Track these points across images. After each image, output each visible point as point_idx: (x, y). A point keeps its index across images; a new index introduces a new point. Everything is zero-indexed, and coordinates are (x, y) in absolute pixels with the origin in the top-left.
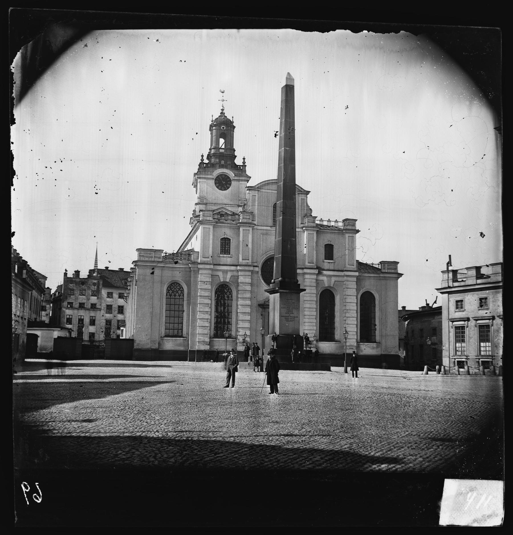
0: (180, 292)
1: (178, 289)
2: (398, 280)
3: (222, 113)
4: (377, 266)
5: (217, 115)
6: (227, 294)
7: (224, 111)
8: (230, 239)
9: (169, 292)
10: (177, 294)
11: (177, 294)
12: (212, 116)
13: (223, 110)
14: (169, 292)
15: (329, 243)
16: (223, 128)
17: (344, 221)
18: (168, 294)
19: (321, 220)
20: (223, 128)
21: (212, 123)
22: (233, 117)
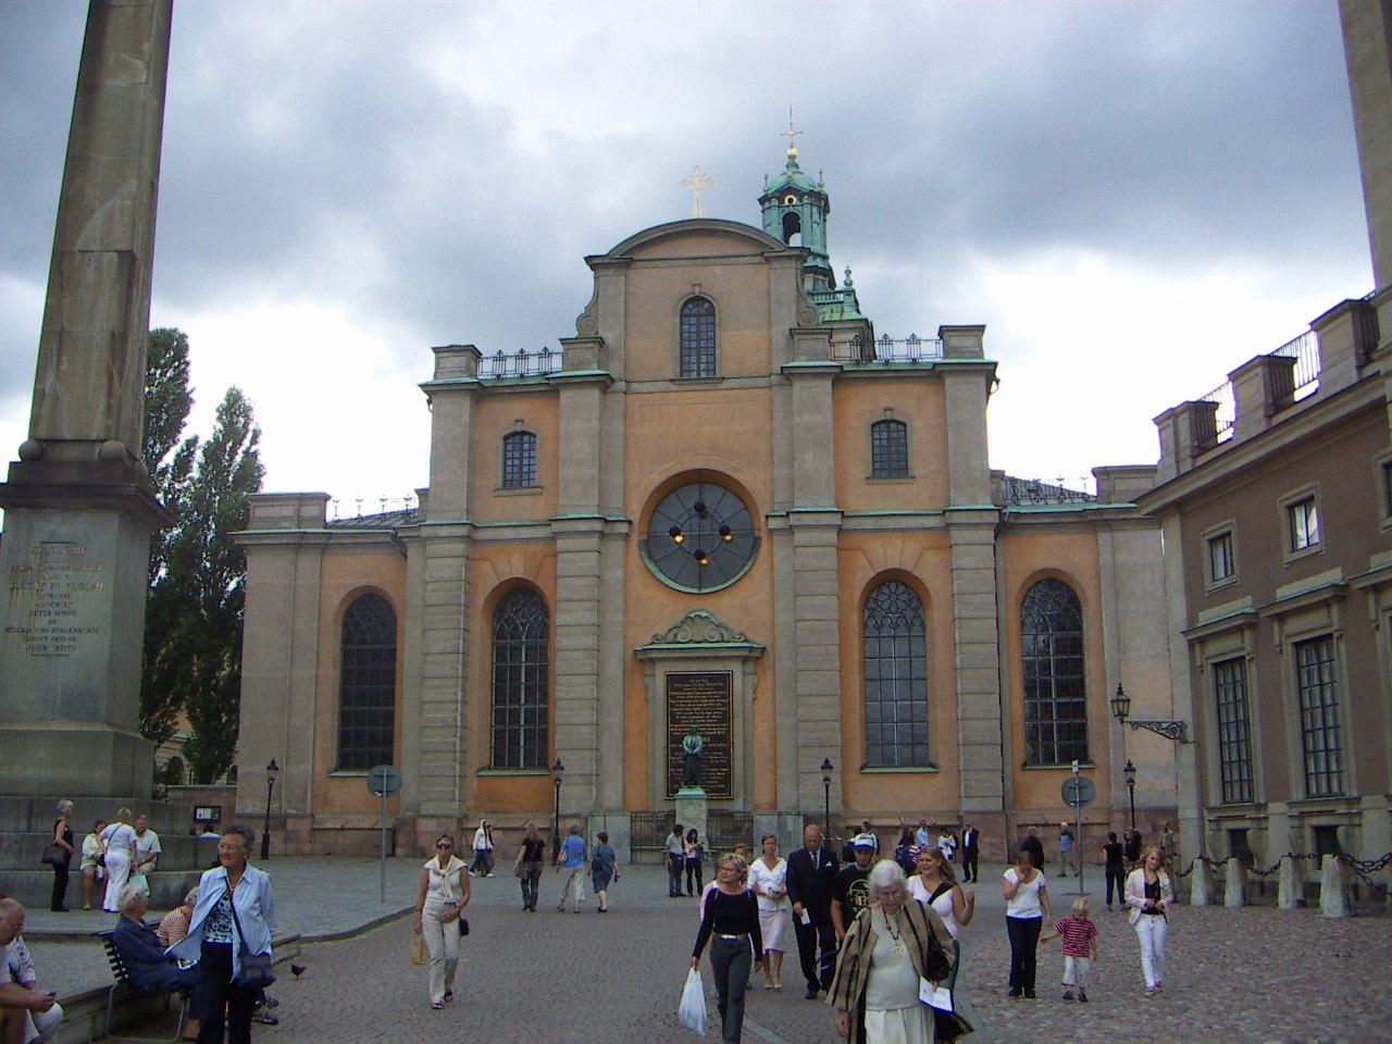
3: (792, 163)
8: (534, 436)
12: (766, 178)
15: (889, 416)
16: (790, 200)
20: (790, 200)
21: (764, 194)
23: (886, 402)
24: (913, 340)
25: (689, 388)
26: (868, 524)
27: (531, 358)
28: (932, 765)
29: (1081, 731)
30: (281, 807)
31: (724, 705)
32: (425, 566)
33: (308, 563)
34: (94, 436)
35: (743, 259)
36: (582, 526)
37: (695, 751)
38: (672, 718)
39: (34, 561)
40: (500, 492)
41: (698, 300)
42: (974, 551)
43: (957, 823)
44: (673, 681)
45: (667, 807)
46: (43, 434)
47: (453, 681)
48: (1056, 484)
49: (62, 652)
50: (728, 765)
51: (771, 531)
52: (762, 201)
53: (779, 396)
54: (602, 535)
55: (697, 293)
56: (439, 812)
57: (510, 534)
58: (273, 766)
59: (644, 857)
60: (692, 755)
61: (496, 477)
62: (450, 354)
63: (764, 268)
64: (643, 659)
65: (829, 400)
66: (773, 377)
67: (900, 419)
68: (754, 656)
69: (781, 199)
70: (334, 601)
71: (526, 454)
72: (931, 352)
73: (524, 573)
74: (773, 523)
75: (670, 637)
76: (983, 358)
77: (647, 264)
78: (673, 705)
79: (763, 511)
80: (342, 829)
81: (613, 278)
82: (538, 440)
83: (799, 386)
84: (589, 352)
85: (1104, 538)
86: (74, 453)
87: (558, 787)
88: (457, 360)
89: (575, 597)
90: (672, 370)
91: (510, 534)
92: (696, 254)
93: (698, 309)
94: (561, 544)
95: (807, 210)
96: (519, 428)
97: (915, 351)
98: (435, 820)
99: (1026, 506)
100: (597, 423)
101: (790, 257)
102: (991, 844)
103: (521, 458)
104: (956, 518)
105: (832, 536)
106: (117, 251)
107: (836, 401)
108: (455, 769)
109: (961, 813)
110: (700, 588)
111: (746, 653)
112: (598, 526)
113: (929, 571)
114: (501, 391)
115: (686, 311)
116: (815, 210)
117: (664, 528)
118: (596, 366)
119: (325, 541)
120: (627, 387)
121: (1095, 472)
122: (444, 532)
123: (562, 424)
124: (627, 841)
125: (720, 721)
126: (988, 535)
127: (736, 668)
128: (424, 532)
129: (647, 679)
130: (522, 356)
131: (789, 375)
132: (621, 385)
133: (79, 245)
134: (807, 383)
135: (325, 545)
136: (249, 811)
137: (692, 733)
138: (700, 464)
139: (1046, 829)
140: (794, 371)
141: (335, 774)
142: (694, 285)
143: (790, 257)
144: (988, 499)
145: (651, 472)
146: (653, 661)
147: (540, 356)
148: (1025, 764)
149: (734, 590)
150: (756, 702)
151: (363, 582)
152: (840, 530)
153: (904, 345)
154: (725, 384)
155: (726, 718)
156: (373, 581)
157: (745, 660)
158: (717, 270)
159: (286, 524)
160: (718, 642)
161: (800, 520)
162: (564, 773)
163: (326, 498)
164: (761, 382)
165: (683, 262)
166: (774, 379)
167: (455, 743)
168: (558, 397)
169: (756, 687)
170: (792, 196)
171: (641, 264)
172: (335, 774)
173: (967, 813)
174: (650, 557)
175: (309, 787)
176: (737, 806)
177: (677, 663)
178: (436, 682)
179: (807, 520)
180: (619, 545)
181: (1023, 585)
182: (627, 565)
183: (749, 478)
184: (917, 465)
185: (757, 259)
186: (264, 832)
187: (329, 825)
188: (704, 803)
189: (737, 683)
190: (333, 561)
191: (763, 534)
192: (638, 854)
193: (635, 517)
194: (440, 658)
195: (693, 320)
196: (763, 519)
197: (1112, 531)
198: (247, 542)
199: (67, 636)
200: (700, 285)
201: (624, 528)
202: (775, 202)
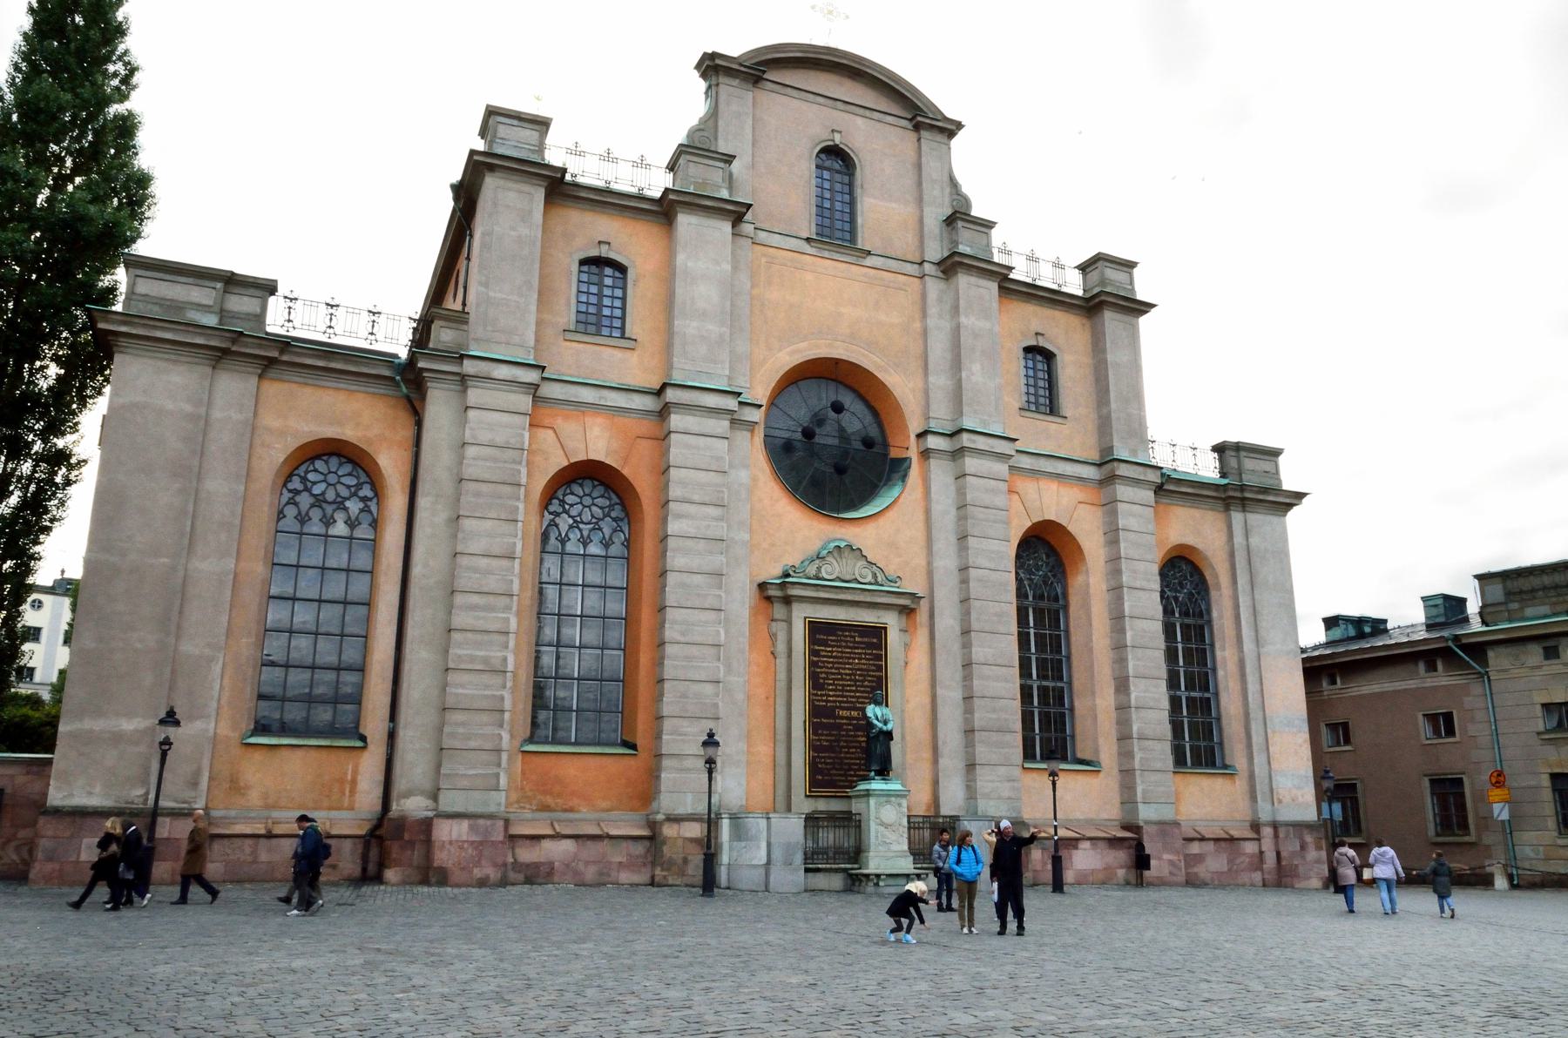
0: (354, 506)
1: (349, 487)
6: (600, 529)
9: (298, 499)
10: (340, 517)
11: (340, 517)
14: (298, 499)
15: (1042, 343)
18: (291, 512)
23: (1036, 326)
24: (1058, 265)
25: (826, 254)
30: (147, 794)
32: (463, 422)
33: (234, 387)
40: (569, 336)
44: (819, 631)
47: (504, 601)
53: (934, 287)
55: (837, 142)
56: (472, 809)
57: (587, 395)
61: (565, 312)
62: (515, 122)
63: (912, 136)
70: (275, 454)
72: (1074, 285)
73: (607, 455)
75: (812, 570)
79: (914, 427)
81: (735, 95)
82: (631, 275)
85: (1237, 517)
88: (528, 133)
89: (696, 498)
90: (808, 230)
91: (587, 395)
93: (836, 158)
94: (676, 420)
96: (604, 252)
98: (465, 824)
102: (1171, 863)
103: (600, 295)
104: (1123, 470)
108: (501, 738)
112: (731, 403)
113: (1085, 527)
114: (583, 194)
119: (275, 354)
121: (1220, 449)
122: (503, 372)
123: (680, 258)
124: (799, 858)
127: (891, 621)
128: (469, 367)
129: (774, 624)
130: (608, 157)
131: (951, 266)
134: (973, 280)
138: (839, 352)
139: (1203, 843)
140: (966, 261)
141: (253, 740)
142: (833, 131)
145: (780, 350)
146: (787, 601)
147: (635, 164)
149: (881, 521)
150: (908, 667)
154: (869, 261)
156: (349, 433)
158: (859, 121)
160: (870, 584)
161: (974, 442)
163: (270, 288)
164: (910, 268)
167: (502, 698)
169: (907, 646)
171: (770, 86)
172: (253, 740)
173: (1147, 822)
175: (206, 763)
177: (818, 607)
178: (475, 599)
179: (982, 443)
183: (901, 384)
189: (894, 638)
190: (276, 390)
191: (913, 454)
194: (484, 562)
197: (1244, 511)
198: (123, 329)
200: (840, 132)
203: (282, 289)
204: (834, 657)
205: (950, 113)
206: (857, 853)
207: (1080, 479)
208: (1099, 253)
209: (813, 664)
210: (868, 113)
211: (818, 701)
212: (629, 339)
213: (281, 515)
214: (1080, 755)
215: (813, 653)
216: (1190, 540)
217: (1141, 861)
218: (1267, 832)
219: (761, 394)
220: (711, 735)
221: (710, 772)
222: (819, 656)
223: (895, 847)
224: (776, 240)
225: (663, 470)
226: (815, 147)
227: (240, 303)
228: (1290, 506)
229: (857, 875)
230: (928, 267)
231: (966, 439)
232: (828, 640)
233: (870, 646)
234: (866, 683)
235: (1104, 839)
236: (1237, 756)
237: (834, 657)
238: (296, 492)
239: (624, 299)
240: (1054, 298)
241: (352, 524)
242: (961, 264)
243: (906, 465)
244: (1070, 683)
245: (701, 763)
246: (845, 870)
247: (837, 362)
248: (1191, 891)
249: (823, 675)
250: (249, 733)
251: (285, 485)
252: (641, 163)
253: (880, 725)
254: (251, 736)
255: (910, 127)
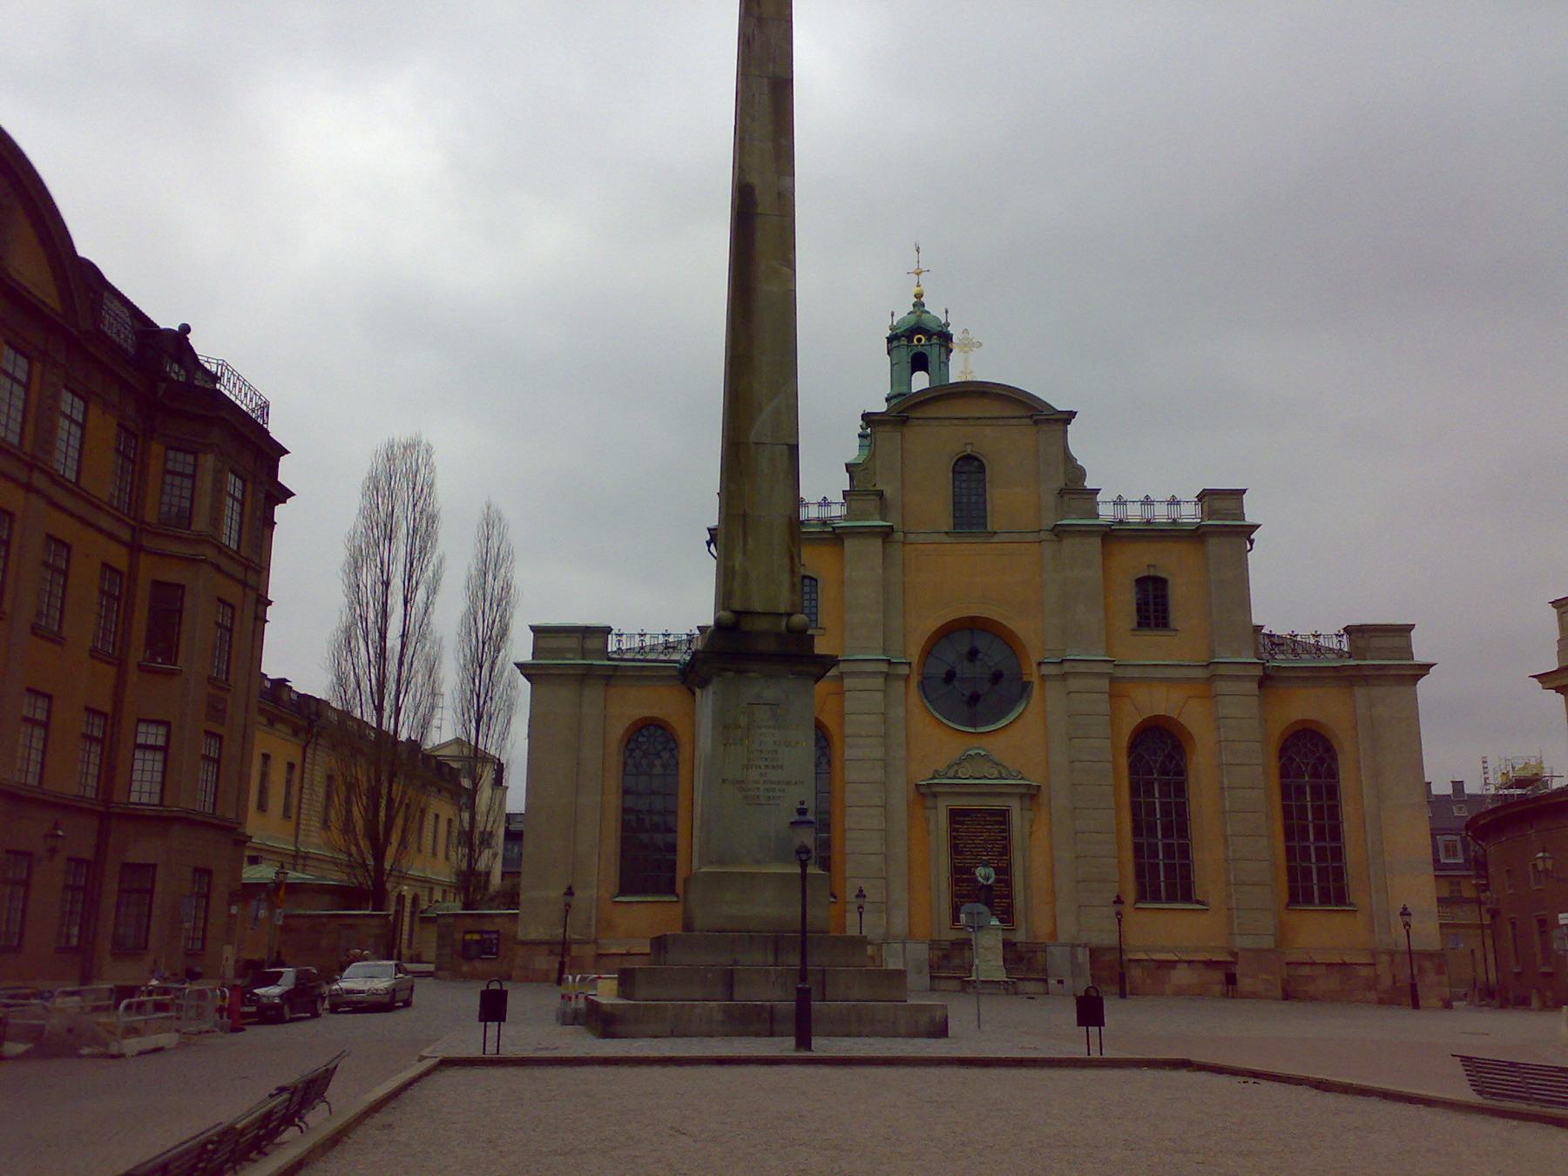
0: (666, 755)
2: (1415, 684)
3: (919, 305)
4: (1334, 643)
5: (903, 310)
7: (922, 299)
8: (816, 580)
10: (658, 762)
11: (658, 762)
12: (892, 315)
13: (919, 296)
15: (1152, 573)
17: (1204, 496)
18: (630, 761)
19: (1120, 502)
20: (919, 340)
22: (947, 312)
24: (1174, 502)
25: (961, 540)
26: (1137, 673)
27: (811, 507)
28: (1198, 902)
29: (1339, 873)
31: (1005, 838)
33: (593, 693)
34: (782, 610)
35: (1011, 420)
36: (870, 667)
37: (989, 882)
38: (955, 849)
39: (743, 720)
41: (969, 458)
42: (1240, 702)
43: (1230, 959)
44: (956, 815)
45: (953, 935)
46: (737, 606)
48: (1312, 641)
49: (771, 802)
50: (1009, 896)
51: (1043, 678)
52: (890, 340)
54: (887, 676)
55: (969, 451)
58: (570, 892)
59: (943, 985)
60: (987, 886)
64: (925, 794)
65: (1099, 557)
66: (1042, 533)
67: (1163, 575)
68: (1031, 795)
69: (910, 339)
70: (618, 729)
71: (807, 597)
72: (1190, 513)
74: (1046, 670)
75: (951, 773)
76: (1244, 520)
77: (921, 422)
78: (955, 838)
79: (1034, 660)
80: (628, 954)
83: (1069, 544)
84: (872, 504)
85: (1360, 692)
86: (762, 624)
87: (861, 914)
90: (946, 523)
92: (965, 415)
93: (969, 468)
94: (848, 683)
95: (936, 350)
97: (1174, 512)
99: (1281, 660)
100: (881, 571)
101: (1056, 421)
104: (1222, 670)
105: (1104, 684)
106: (787, 445)
107: (1106, 556)
109: (1236, 950)
110: (974, 726)
111: (1024, 790)
112: (884, 667)
115: (958, 469)
116: (943, 349)
117: (941, 671)
118: (878, 517)
119: (611, 673)
120: (905, 537)
124: (926, 969)
125: (1001, 854)
126: (1255, 686)
127: (1015, 806)
132: (899, 536)
133: (752, 439)
135: (610, 676)
136: (533, 936)
137: (985, 865)
138: (974, 612)
141: (617, 899)
143: (1056, 421)
144: (1252, 654)
146: (935, 795)
147: (820, 505)
148: (1288, 905)
151: (646, 713)
152: (1113, 680)
153: (1164, 506)
154: (996, 539)
155: (1006, 850)
156: (656, 712)
157: (1022, 796)
158: (988, 430)
159: (569, 656)
162: (866, 900)
163: (608, 630)
164: (1031, 537)
165: (955, 422)
166: (1043, 535)
168: (843, 543)
169: (1032, 821)
170: (919, 336)
172: (617, 899)
173: (1243, 950)
174: (926, 697)
175: (594, 912)
176: (1020, 936)
179: (1081, 668)
180: (899, 687)
181: (1282, 734)
182: (911, 706)
184: (1176, 615)
185: (1028, 420)
186: (560, 959)
187: (613, 951)
188: (1000, 932)
189: (1016, 818)
191: (1035, 679)
192: (937, 981)
193: (915, 659)
195: (964, 477)
196: (1034, 665)
199: (777, 787)
201: (905, 670)
202: (904, 341)
203: (615, 631)
204: (970, 832)
205: (1061, 406)
206: (969, 968)
207: (1189, 679)
208: (1204, 490)
209: (953, 838)
210: (994, 422)
211: (959, 863)
212: (821, 628)
213: (625, 764)
214: (1197, 898)
215: (953, 830)
216: (1310, 715)
217: (1231, 979)
218: (1384, 959)
219: (914, 655)
220: (861, 891)
221: (861, 914)
222: (958, 832)
223: (993, 963)
224: (922, 538)
225: (842, 715)
226: (952, 459)
227: (593, 643)
228: (1418, 677)
229: (968, 981)
230: (1043, 535)
231: (1067, 667)
232: (965, 821)
233: (996, 823)
234: (995, 849)
235: (1199, 962)
236: (1355, 895)
237: (970, 832)
238: (633, 750)
239: (816, 600)
240: (1171, 533)
241: (664, 766)
242: (1065, 531)
243: (1030, 687)
244: (1191, 841)
245: (855, 907)
246: (960, 978)
247: (973, 619)
248: (1286, 1005)
249: (962, 845)
250: (615, 895)
251: (626, 746)
252: (825, 503)
253: (982, 880)
254: (616, 897)
255: (1031, 423)
